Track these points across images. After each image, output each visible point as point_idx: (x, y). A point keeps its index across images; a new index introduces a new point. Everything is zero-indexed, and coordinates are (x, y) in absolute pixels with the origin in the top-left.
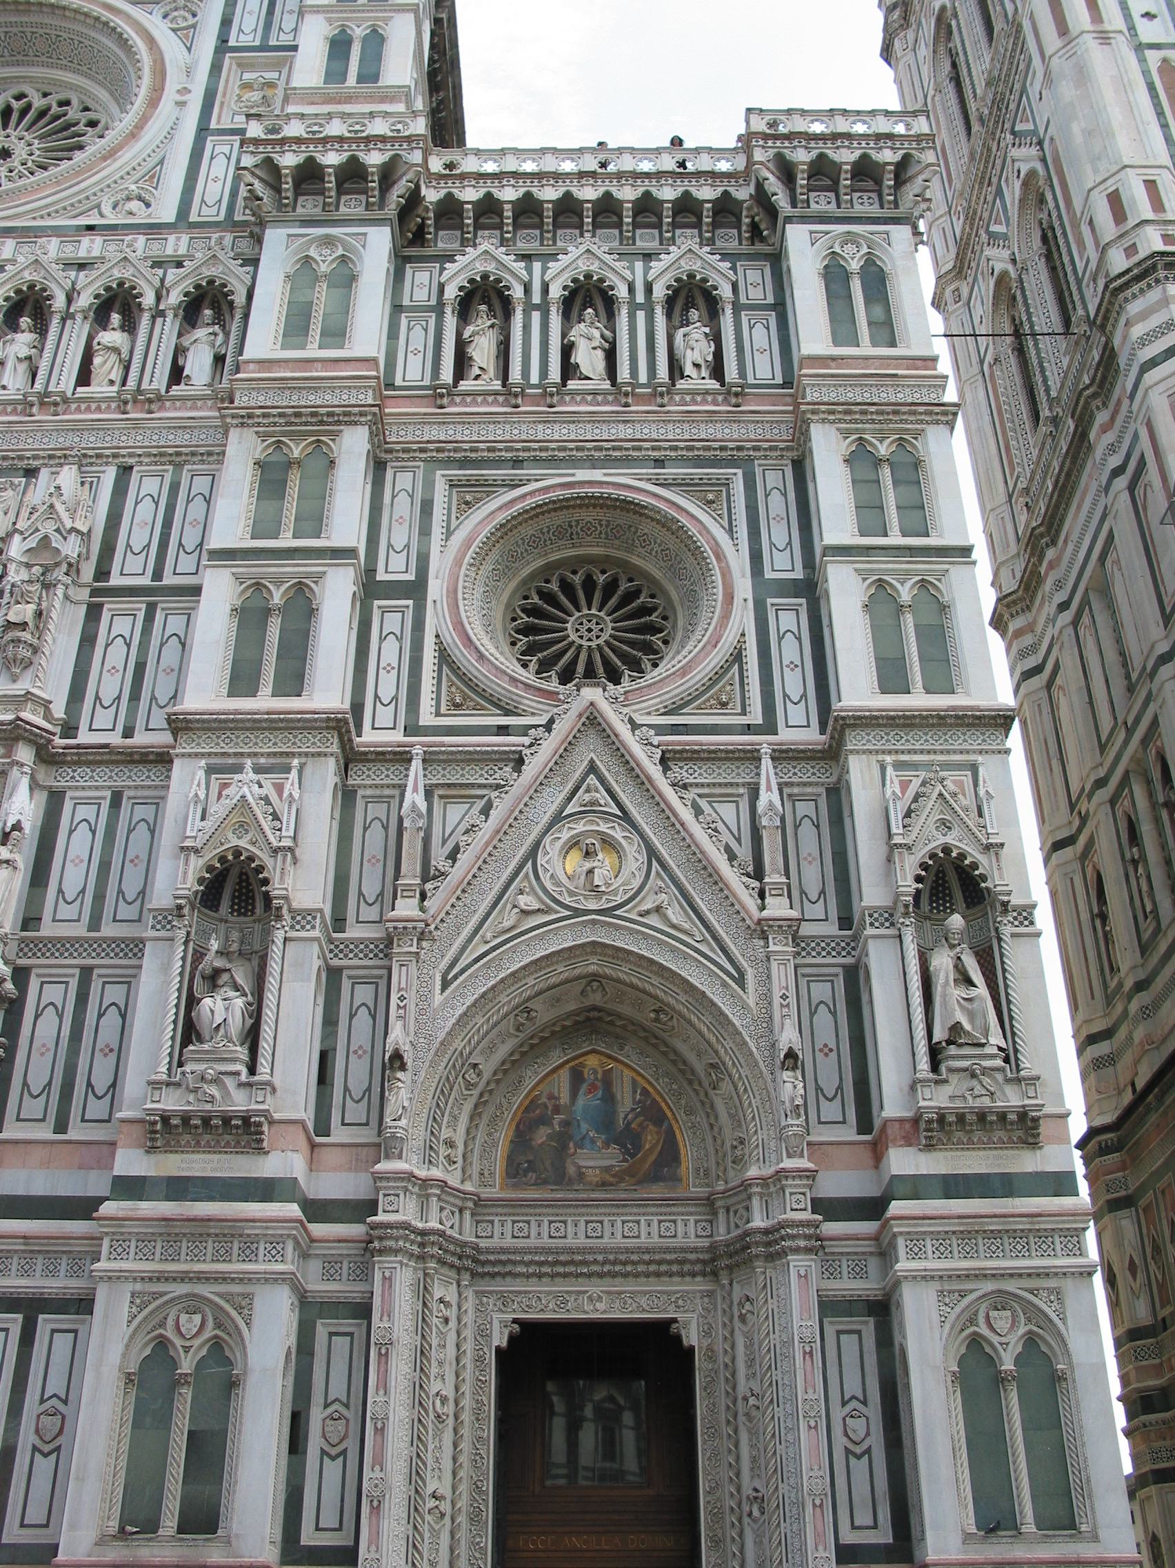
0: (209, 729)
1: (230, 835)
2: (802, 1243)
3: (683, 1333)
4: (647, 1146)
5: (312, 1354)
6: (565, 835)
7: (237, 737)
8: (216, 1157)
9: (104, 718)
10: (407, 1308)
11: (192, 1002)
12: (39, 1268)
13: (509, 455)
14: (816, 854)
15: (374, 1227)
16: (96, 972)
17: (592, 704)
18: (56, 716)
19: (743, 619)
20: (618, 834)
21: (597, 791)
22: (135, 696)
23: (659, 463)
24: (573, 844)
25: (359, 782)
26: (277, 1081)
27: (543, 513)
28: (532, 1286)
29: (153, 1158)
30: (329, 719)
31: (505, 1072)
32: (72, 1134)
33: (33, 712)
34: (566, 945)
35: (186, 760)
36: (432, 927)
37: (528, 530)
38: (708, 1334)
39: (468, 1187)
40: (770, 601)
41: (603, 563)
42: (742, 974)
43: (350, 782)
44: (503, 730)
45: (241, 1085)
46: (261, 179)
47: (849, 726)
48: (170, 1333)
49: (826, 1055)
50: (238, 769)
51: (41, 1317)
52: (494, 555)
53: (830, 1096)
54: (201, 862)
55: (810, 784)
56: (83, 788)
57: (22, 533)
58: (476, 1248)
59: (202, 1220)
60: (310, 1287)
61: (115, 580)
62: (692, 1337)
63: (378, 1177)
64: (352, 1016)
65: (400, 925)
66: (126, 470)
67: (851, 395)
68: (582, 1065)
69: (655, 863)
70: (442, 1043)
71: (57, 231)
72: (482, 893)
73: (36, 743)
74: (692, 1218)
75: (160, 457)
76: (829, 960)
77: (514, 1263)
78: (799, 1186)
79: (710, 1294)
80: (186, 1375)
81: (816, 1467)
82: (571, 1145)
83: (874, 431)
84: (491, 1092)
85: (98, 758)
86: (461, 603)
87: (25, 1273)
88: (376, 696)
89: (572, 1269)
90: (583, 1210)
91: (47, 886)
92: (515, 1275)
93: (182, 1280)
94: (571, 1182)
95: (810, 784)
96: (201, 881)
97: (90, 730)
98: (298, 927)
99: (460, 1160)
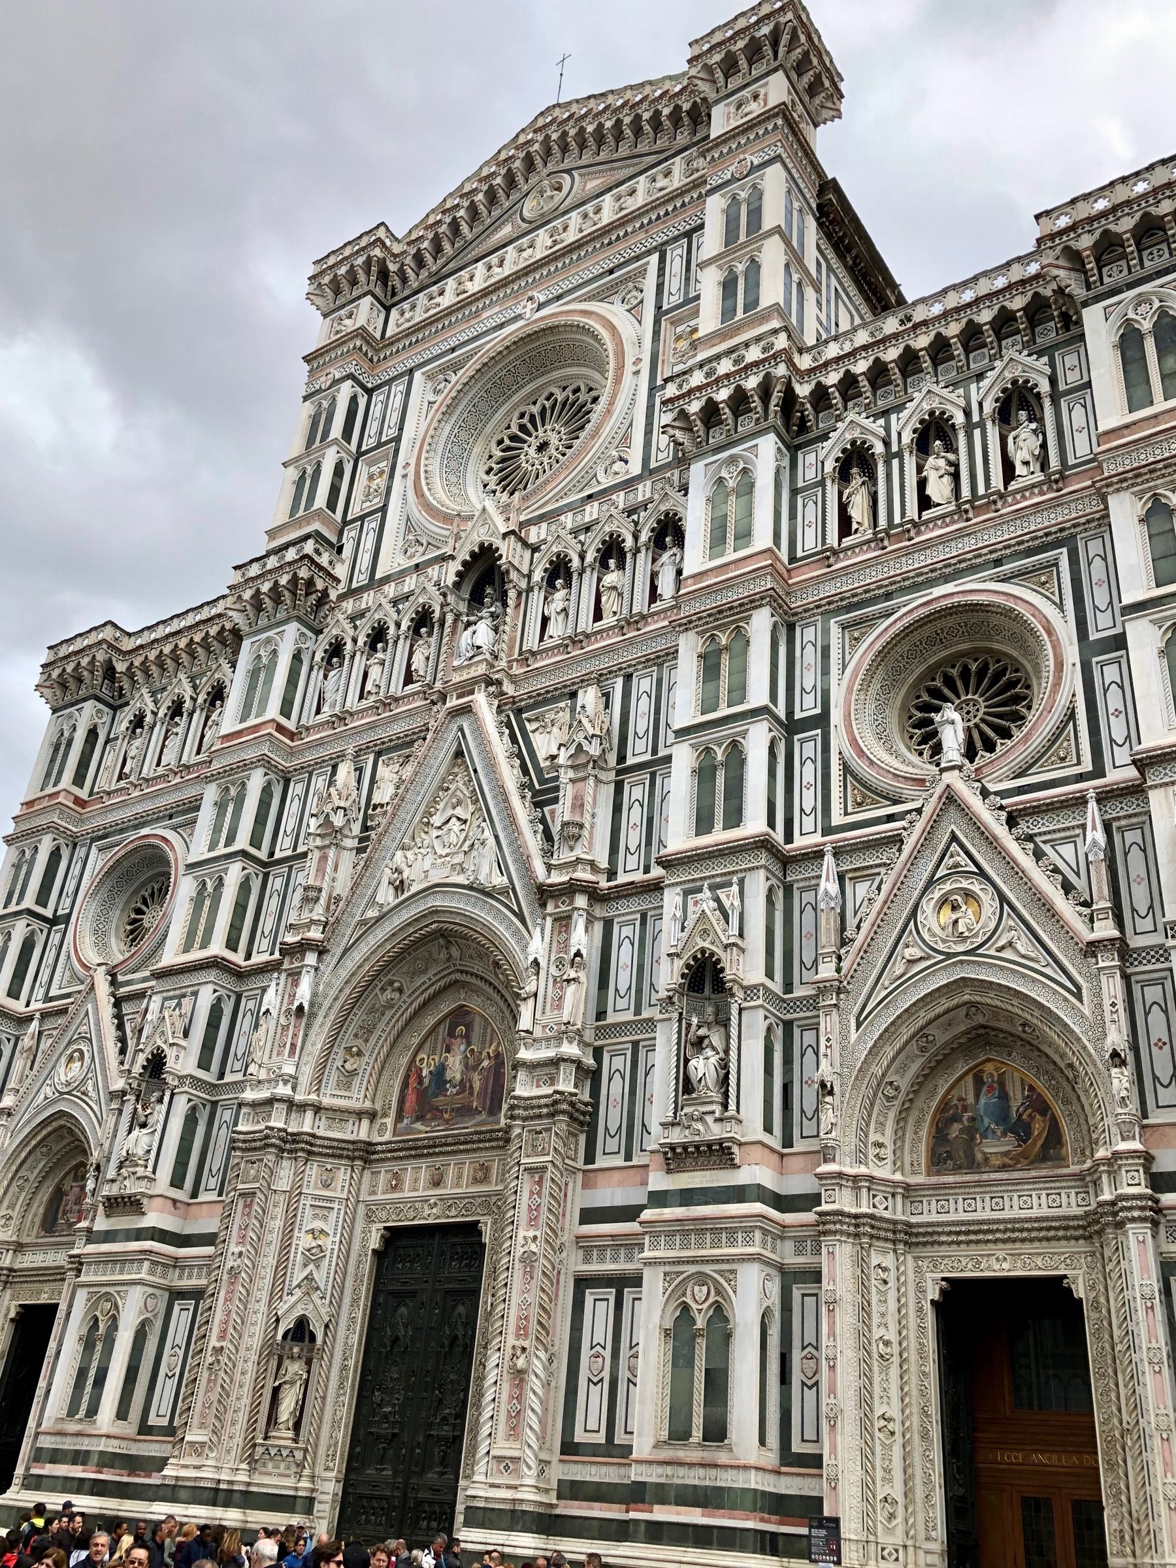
1: (698, 940)
2: (1136, 1214)
3: (1073, 1287)
5: (791, 1310)
6: (937, 895)
9: (632, 861)
10: (848, 1274)
11: (687, 1061)
12: (622, 1256)
13: (881, 591)
14: (1144, 874)
15: (820, 1214)
16: (641, 1044)
17: (948, 786)
18: (602, 867)
19: (1074, 681)
20: (976, 887)
21: (959, 855)
22: (649, 843)
23: (998, 563)
24: (943, 901)
25: (794, 878)
26: (742, 1116)
27: (912, 632)
28: (953, 1250)
30: (755, 842)
31: (921, 1084)
33: (584, 870)
34: (942, 983)
36: (845, 983)
37: (904, 648)
38: (1093, 1288)
39: (898, 1177)
40: (1095, 660)
41: (973, 654)
42: (1079, 988)
43: (788, 879)
44: (890, 818)
45: (717, 1120)
46: (680, 428)
47: (1147, 765)
48: (689, 1300)
49: (1161, 1048)
50: (700, 890)
52: (880, 674)
53: (1165, 1084)
54: (682, 962)
55: (1135, 815)
56: (624, 915)
58: (909, 1225)
60: (786, 1261)
61: (630, 761)
62: (1080, 1291)
63: (820, 1177)
64: (802, 1056)
65: (821, 985)
66: (628, 677)
67: (1146, 457)
68: (982, 1071)
69: (1006, 907)
70: (860, 1071)
71: (570, 508)
72: (880, 950)
74: (1073, 1191)
75: (647, 662)
76: (1159, 966)
77: (939, 1234)
78: (1132, 1164)
79: (1093, 1254)
81: (1161, 1406)
83: (1163, 485)
84: (910, 1100)
86: (854, 723)
87: (615, 1260)
88: (802, 810)
89: (981, 1237)
90: (988, 1189)
92: (941, 1243)
93: (693, 1262)
94: (979, 1166)
95: (1135, 815)
96: (683, 976)
99: (890, 1158)
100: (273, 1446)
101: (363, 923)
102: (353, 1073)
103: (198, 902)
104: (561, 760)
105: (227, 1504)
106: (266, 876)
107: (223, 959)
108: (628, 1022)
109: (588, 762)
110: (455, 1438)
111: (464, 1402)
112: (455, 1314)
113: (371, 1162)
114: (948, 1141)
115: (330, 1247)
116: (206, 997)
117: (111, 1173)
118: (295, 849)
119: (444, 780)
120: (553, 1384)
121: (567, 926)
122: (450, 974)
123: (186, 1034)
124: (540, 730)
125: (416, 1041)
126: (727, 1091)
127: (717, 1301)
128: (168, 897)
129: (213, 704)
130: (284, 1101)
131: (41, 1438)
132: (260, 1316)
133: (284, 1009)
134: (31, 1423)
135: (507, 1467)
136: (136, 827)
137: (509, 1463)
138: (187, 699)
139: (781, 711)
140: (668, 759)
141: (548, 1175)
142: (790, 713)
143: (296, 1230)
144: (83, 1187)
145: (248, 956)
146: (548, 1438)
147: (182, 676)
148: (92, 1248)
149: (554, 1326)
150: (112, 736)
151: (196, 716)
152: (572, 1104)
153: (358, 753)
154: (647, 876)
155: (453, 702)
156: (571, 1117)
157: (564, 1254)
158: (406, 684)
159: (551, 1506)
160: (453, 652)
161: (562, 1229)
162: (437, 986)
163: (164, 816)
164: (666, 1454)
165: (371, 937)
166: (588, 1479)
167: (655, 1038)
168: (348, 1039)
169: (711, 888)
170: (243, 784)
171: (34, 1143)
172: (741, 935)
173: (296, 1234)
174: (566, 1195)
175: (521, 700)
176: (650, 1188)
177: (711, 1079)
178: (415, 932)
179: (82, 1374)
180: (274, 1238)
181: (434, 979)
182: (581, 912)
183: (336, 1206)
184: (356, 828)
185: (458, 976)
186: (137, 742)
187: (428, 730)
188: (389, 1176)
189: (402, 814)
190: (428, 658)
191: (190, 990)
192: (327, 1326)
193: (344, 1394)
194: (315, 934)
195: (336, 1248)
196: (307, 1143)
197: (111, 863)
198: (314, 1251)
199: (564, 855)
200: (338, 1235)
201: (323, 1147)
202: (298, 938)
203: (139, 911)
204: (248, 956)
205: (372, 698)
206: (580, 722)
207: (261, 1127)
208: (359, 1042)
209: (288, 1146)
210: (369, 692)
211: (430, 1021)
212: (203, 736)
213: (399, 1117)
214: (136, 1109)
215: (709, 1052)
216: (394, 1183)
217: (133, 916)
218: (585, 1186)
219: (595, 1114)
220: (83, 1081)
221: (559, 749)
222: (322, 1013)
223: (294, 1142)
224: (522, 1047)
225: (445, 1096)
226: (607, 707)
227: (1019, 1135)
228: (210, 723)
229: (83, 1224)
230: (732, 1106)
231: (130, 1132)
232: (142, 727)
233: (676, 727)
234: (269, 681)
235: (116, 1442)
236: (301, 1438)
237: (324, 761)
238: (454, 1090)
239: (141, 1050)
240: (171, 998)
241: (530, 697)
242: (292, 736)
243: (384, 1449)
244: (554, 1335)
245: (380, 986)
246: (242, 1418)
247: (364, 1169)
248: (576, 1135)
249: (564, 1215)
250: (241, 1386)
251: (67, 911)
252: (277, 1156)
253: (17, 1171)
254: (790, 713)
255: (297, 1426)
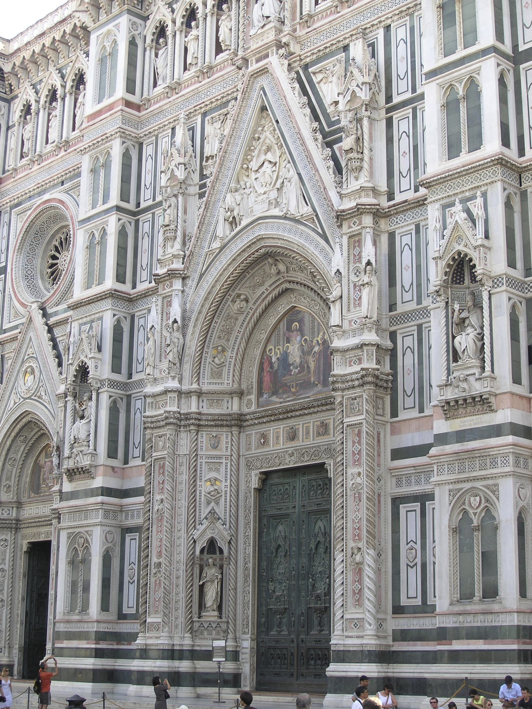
0: (440, 183)
7: (454, 184)
8: (474, 417)
9: (405, 184)
11: (454, 337)
16: (424, 326)
22: (416, 167)
25: (528, 184)
29: (449, 422)
30: (492, 161)
32: (427, 412)
33: (367, 196)
35: (433, 204)
45: (476, 380)
50: (452, 204)
51: (427, 503)
54: (444, 263)
57: (342, 94)
59: (471, 451)
61: (396, 100)
66: (388, 28)
73: (371, 212)
80: (476, 526)
85: (405, 208)
87: (418, 483)
91: (396, 285)
96: (446, 274)
97: (400, 192)
98: (496, 286)
100: (205, 621)
101: (210, 252)
102: (221, 365)
103: (90, 247)
104: (341, 107)
105: (181, 658)
106: (137, 221)
107: (115, 290)
108: (413, 311)
109: (362, 105)
110: (326, 608)
111: (329, 585)
112: (317, 527)
113: (244, 427)
115: (224, 489)
116: (108, 322)
117: (67, 453)
118: (154, 199)
119: (255, 131)
120: (383, 570)
121: (359, 241)
122: (281, 284)
123: (100, 349)
124: (324, 80)
125: (264, 336)
126: (484, 357)
127: (487, 506)
128: (71, 246)
129: (78, 88)
130: (175, 391)
131: (57, 625)
132: (182, 540)
133: (164, 324)
134: (50, 617)
135: (356, 625)
136: (40, 194)
137: (358, 623)
138: (59, 87)
139: (507, 48)
140: (422, 97)
141: (364, 429)
142: (515, 47)
143: (198, 480)
144: (52, 462)
145: (134, 287)
146: (383, 604)
147: (52, 68)
148: (64, 504)
149: (380, 531)
150: (10, 124)
151: (67, 99)
152: (377, 377)
153: (188, 116)
154: (418, 194)
155: (254, 67)
156: (377, 385)
157: (382, 482)
158: (217, 54)
159: (389, 646)
160: (249, 24)
161: (379, 465)
162: (273, 295)
163: (58, 184)
164: (457, 608)
165: (218, 263)
166: (412, 628)
167: (430, 322)
168: (214, 339)
169: (461, 202)
170: (108, 153)
171: (13, 434)
172: (487, 237)
173: (198, 483)
174: (379, 441)
175: (307, 57)
176: (435, 432)
177: (471, 350)
178: (249, 256)
179: (74, 585)
180: (184, 488)
181: (270, 289)
182: (368, 230)
183: (224, 461)
184: (196, 177)
185: (287, 285)
186: (29, 127)
187: (237, 90)
188: (258, 436)
189: (227, 164)
190: (231, 30)
191: (97, 315)
192: (230, 543)
193: (249, 586)
194: (177, 265)
195: (228, 489)
196: (195, 419)
197: (27, 225)
198: (212, 494)
199: (353, 185)
200: (229, 481)
201: (208, 420)
202: (165, 270)
203: (54, 257)
204: (134, 287)
205: (193, 69)
206: (352, 72)
207: (161, 411)
208: (223, 342)
209: (183, 423)
210: (190, 64)
211: (272, 320)
212: (75, 116)
213: (260, 394)
214: (75, 407)
215: (469, 330)
216: (262, 441)
217: (51, 261)
218: (393, 433)
219: (395, 381)
220: (37, 389)
221: (338, 96)
222: (191, 324)
223: (187, 419)
224: (336, 338)
225: (291, 375)
226: (373, 56)
228: (78, 105)
229: (56, 488)
230: (488, 368)
231: (74, 423)
232: (31, 114)
233: (426, 70)
234: (114, 67)
235: (104, 625)
236: (224, 616)
237: (165, 126)
238: (297, 371)
239: (71, 364)
240: (85, 324)
241: (313, 54)
242: (138, 108)
243: (280, 618)
244: (380, 537)
245: (231, 299)
246: (182, 604)
247: (240, 432)
248: (382, 398)
249: (379, 455)
250: (177, 586)
251: (4, 264)
252: (176, 431)
253: (7, 455)
254: (515, 47)
255: (220, 608)
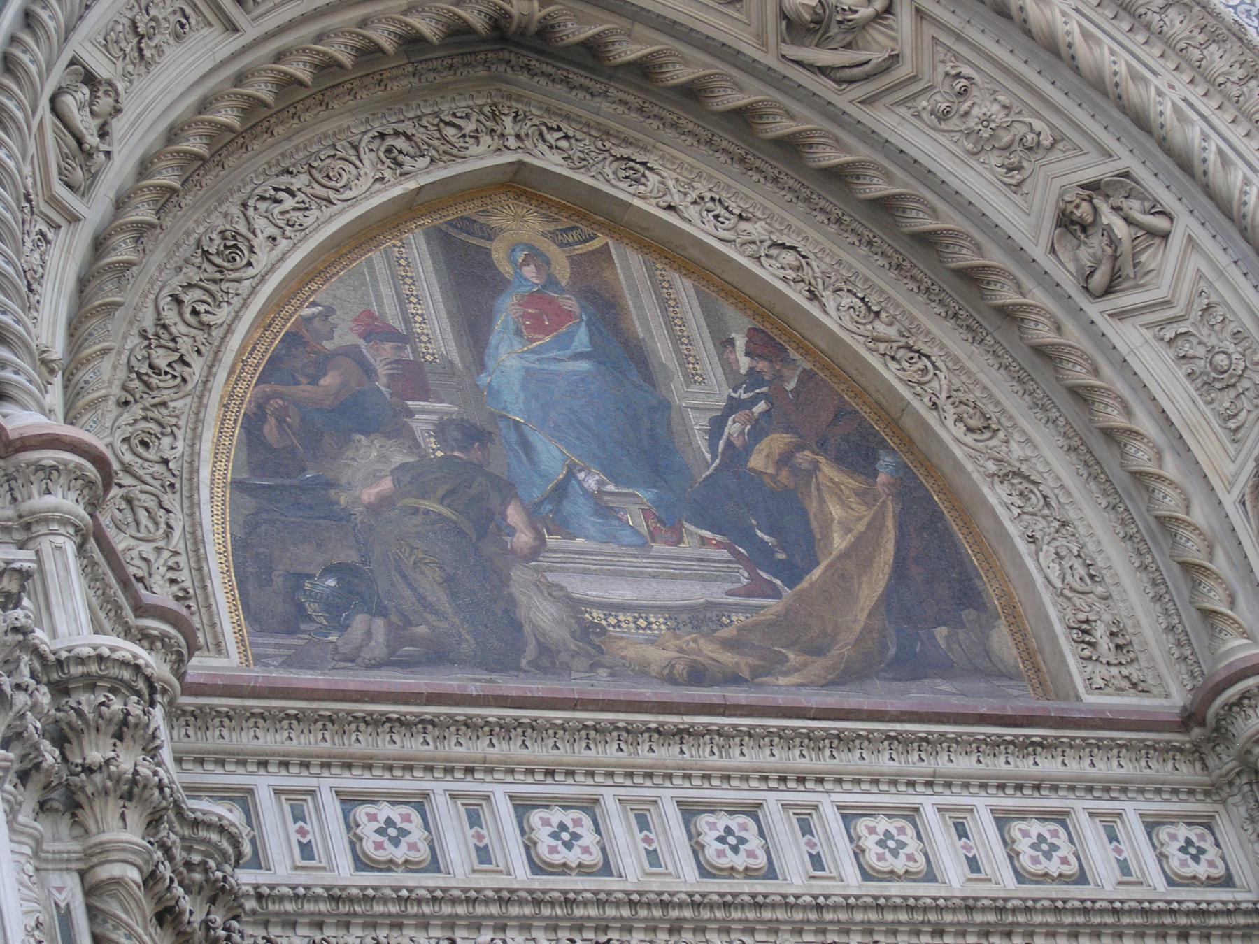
4: (839, 542)
82: (514, 515)
90: (667, 754)
114: (342, 518)
227: (747, 537)
